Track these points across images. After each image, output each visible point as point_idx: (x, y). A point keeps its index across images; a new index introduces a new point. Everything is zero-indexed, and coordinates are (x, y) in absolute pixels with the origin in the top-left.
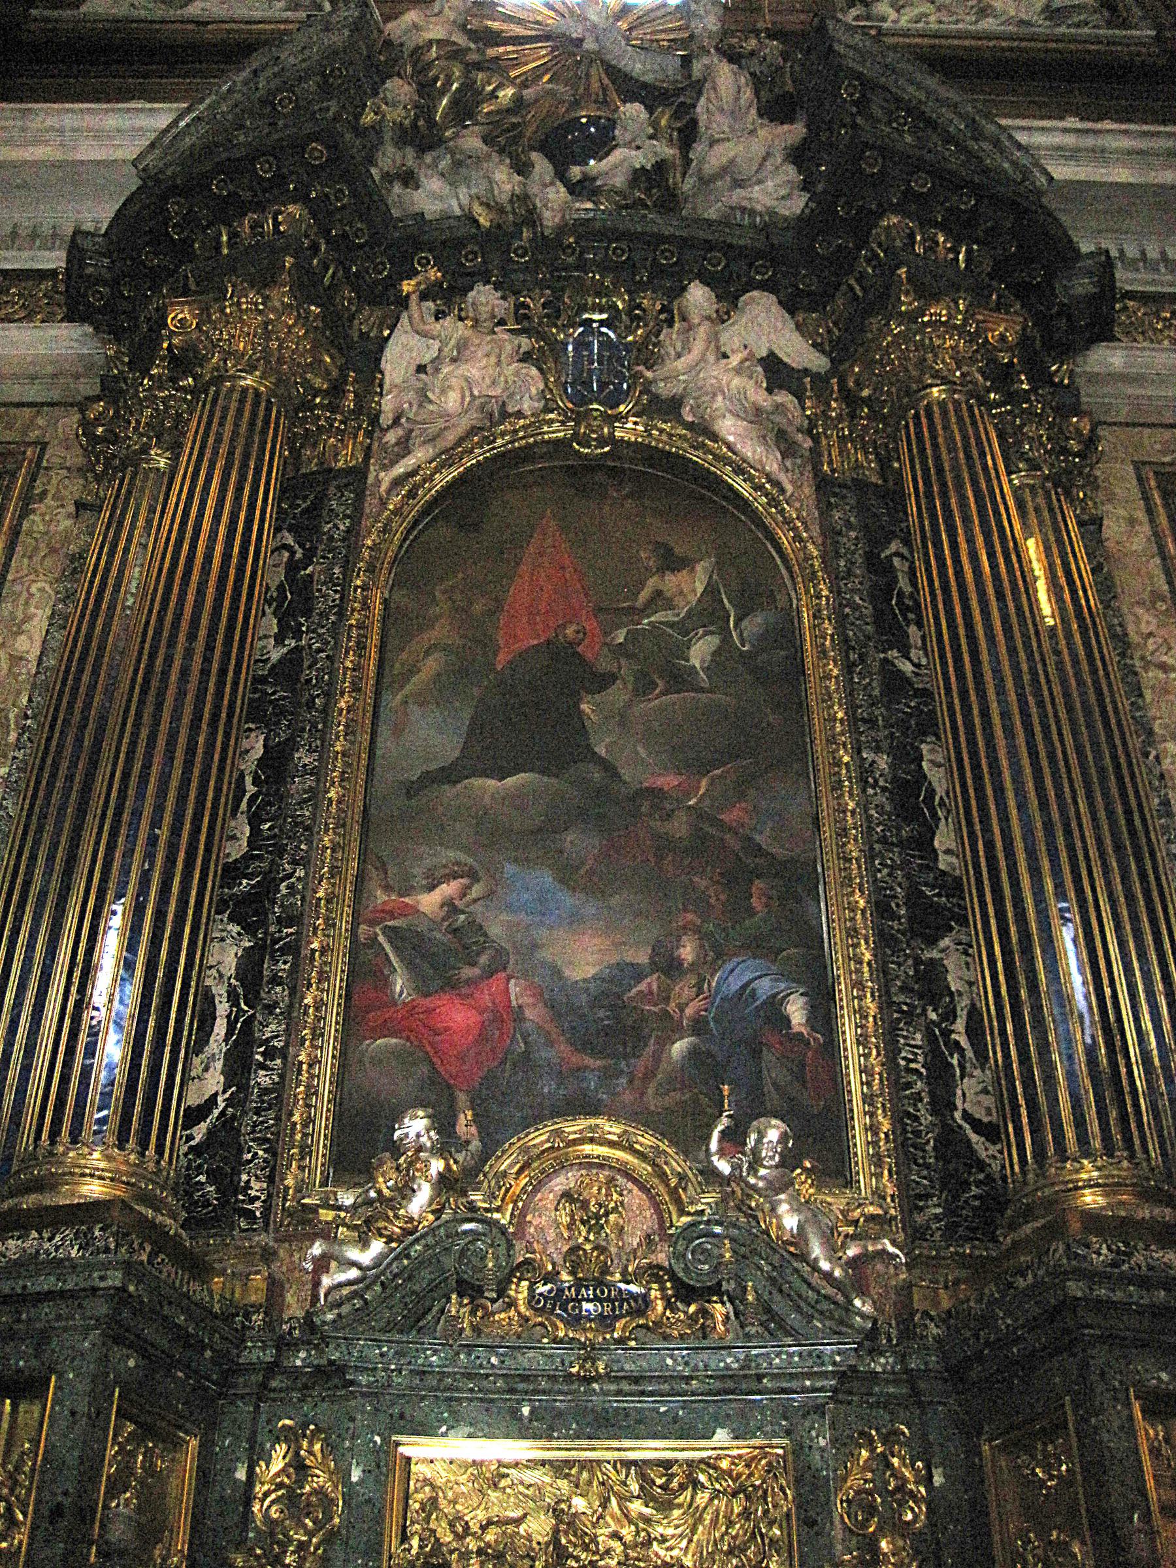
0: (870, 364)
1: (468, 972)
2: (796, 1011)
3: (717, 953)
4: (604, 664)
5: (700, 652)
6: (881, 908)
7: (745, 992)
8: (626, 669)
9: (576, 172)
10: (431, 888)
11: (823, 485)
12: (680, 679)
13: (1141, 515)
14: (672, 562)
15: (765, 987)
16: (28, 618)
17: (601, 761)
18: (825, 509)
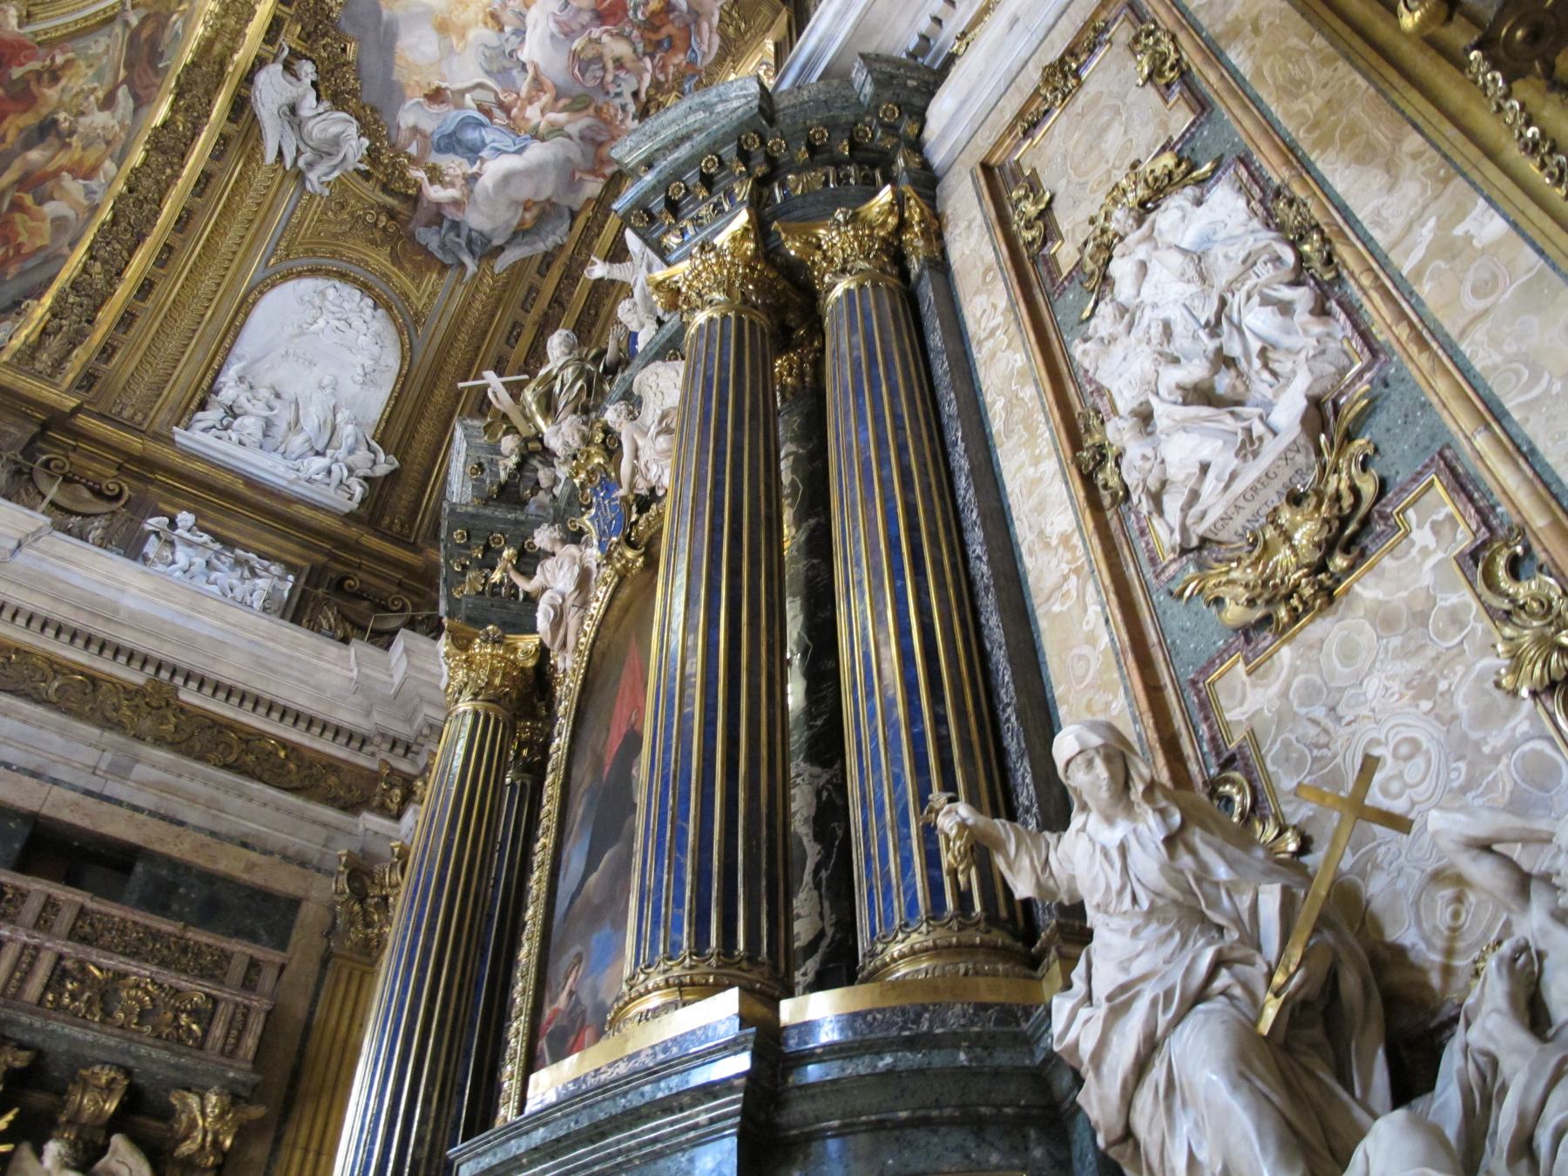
13: (976, 213)
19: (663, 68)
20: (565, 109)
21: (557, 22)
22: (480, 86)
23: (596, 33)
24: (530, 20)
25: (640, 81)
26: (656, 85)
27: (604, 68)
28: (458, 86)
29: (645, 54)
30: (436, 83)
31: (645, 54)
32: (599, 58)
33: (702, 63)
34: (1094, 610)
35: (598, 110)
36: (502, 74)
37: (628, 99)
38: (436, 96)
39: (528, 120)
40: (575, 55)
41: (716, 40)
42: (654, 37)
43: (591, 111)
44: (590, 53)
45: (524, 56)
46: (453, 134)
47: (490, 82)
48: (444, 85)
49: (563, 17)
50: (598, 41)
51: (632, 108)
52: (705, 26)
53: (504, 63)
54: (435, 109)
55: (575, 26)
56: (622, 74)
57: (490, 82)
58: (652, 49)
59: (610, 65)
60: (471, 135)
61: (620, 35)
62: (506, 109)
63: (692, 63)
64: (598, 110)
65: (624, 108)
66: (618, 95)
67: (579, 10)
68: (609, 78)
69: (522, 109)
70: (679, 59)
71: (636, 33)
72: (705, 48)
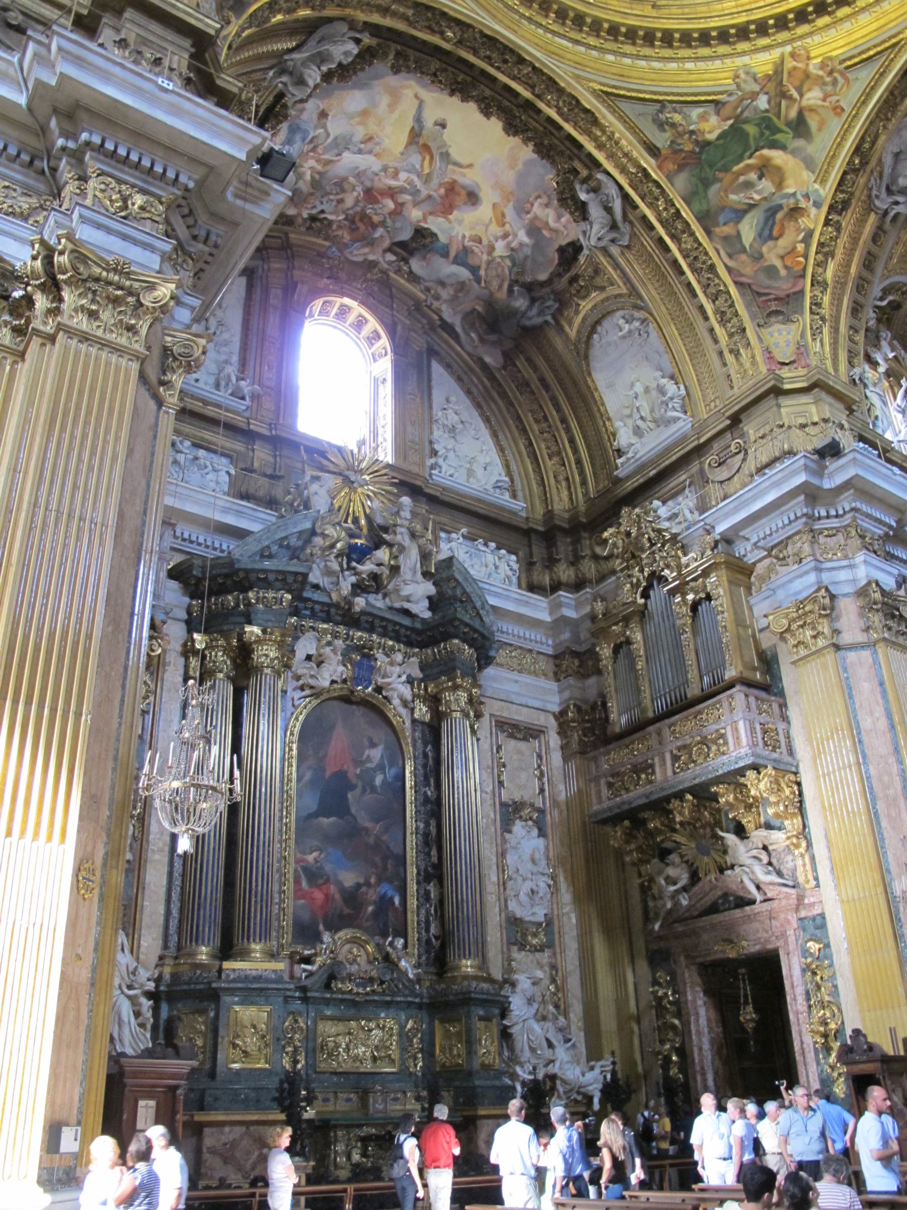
0: (436, 686)
1: (321, 881)
2: (397, 901)
3: (380, 881)
4: (354, 781)
5: (379, 780)
6: (418, 874)
7: (385, 895)
8: (360, 784)
9: (354, 564)
10: (311, 853)
11: (414, 721)
12: (373, 789)
14: (373, 745)
15: (390, 893)
16: (171, 721)
17: (352, 815)
18: (414, 730)
19: (340, 227)
20: (312, 177)
21: (365, 170)
22: (328, 135)
23: (359, 189)
24: (367, 156)
25: (331, 213)
26: (330, 223)
27: (337, 194)
28: (329, 125)
29: (347, 215)
30: (331, 114)
31: (347, 215)
32: (343, 191)
33: (347, 253)
34: (497, 909)
35: (312, 194)
36: (336, 143)
37: (320, 208)
38: (323, 115)
39: (306, 161)
40: (345, 179)
41: (360, 259)
42: (357, 219)
43: (312, 191)
44: (346, 186)
45: (346, 154)
46: (299, 128)
47: (330, 140)
48: (330, 118)
49: (369, 173)
50: (354, 190)
51: (314, 212)
52: (367, 250)
53: (342, 145)
54: (315, 116)
55: (363, 179)
56: (334, 203)
57: (330, 140)
58: (351, 220)
59: (339, 197)
60: (298, 137)
61: (357, 201)
62: (314, 150)
63: (346, 246)
64: (312, 194)
65: (314, 207)
66: (322, 203)
67: (372, 181)
68: (332, 197)
69: (312, 158)
70: (347, 237)
71: (358, 209)
72: (355, 252)
